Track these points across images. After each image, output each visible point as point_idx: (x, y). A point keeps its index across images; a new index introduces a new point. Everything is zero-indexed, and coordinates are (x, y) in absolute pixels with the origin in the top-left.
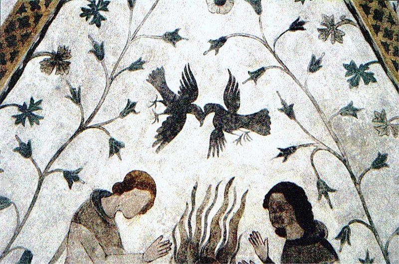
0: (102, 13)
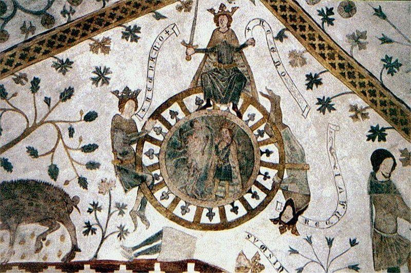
0: (393, 61)
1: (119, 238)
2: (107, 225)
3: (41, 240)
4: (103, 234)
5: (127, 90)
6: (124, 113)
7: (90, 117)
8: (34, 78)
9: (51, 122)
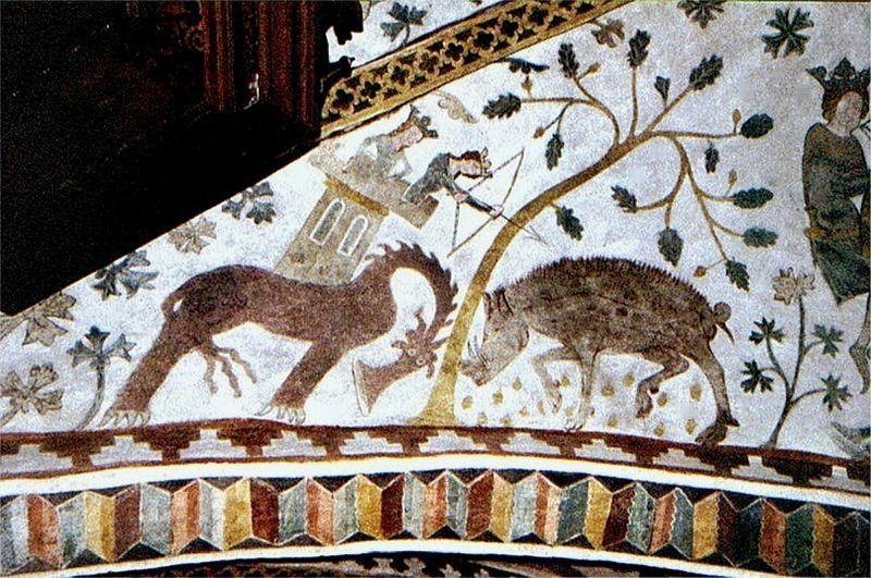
1: (828, 403)
2: (797, 369)
3: (649, 392)
4: (790, 392)
5: (845, 66)
6: (835, 121)
7: (756, 127)
8: (639, 32)
9: (666, 134)
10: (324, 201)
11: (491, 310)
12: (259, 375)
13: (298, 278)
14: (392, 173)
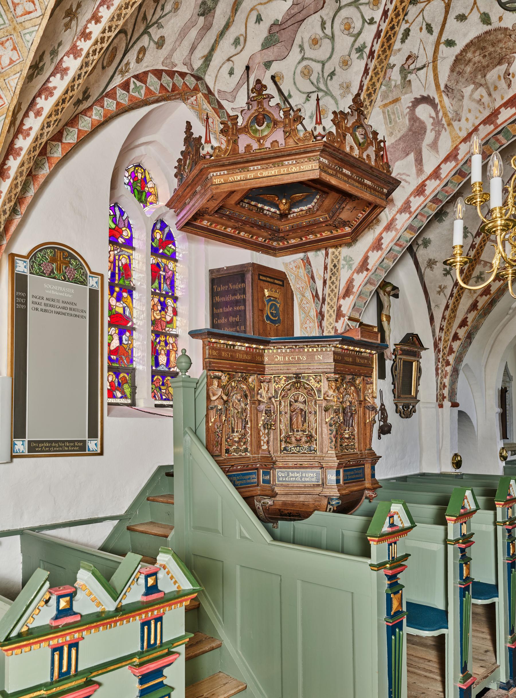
10: (384, 112)
11: (447, 95)
12: (409, 174)
13: (396, 139)
14: (393, 87)
